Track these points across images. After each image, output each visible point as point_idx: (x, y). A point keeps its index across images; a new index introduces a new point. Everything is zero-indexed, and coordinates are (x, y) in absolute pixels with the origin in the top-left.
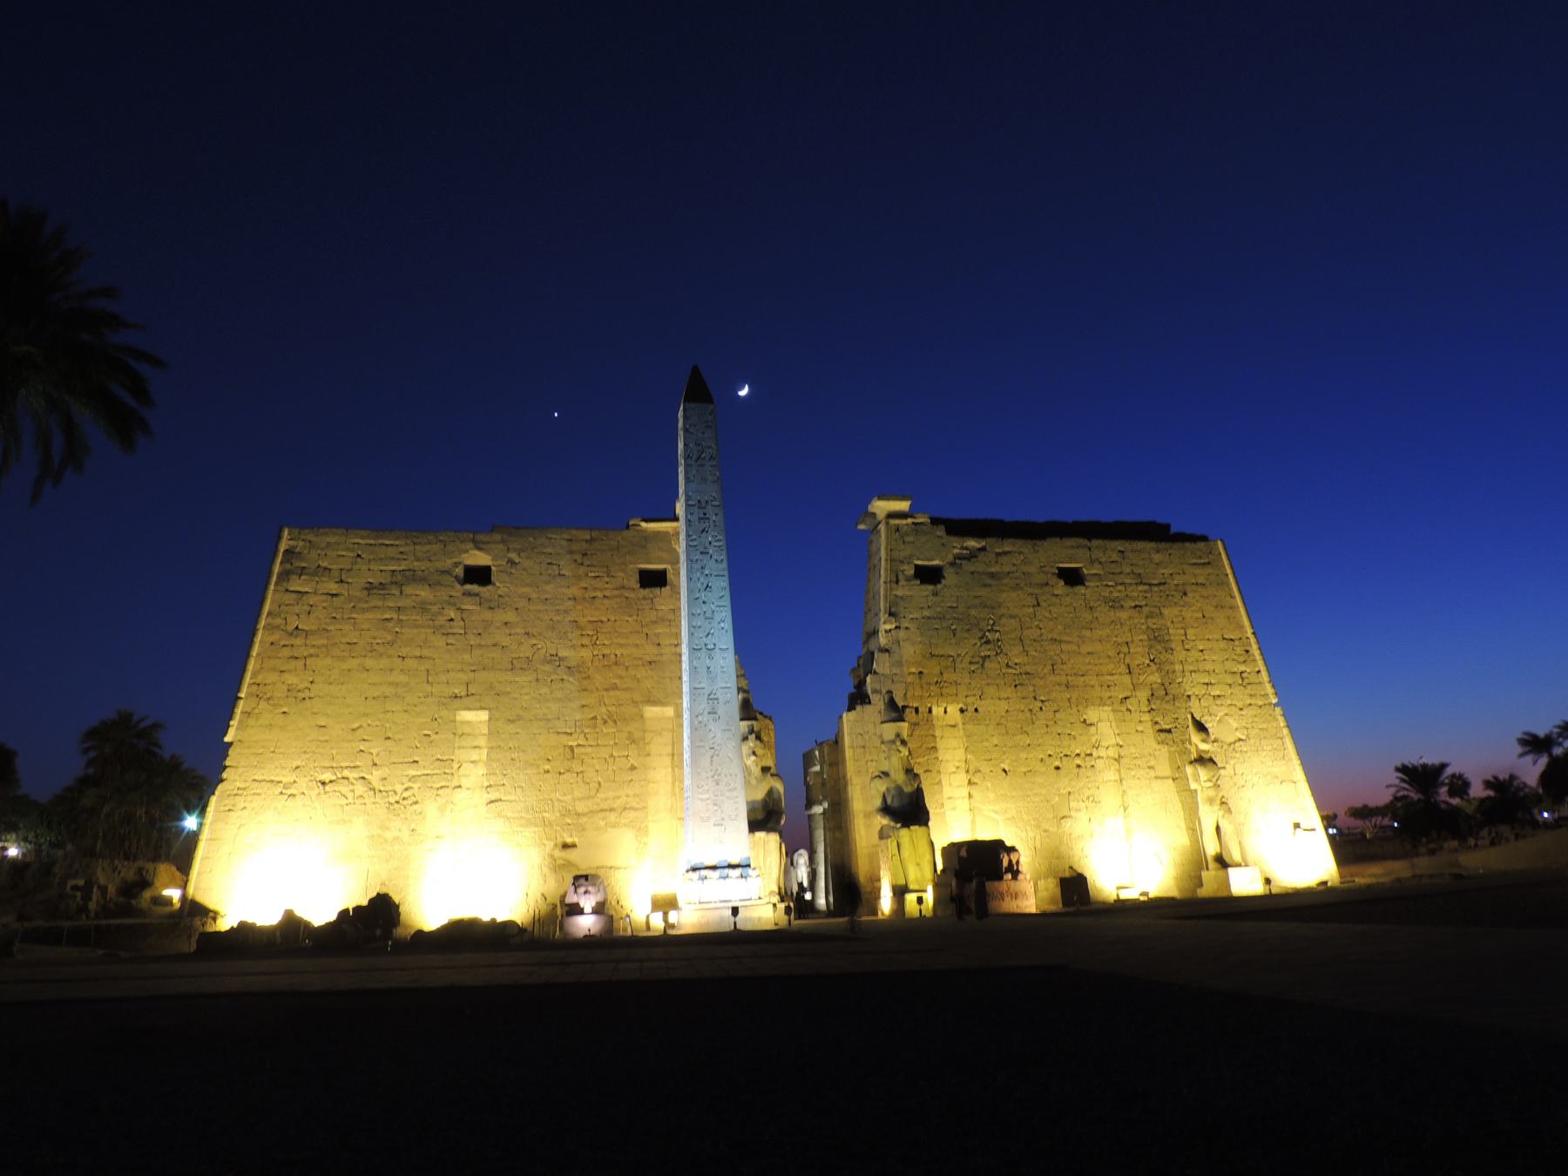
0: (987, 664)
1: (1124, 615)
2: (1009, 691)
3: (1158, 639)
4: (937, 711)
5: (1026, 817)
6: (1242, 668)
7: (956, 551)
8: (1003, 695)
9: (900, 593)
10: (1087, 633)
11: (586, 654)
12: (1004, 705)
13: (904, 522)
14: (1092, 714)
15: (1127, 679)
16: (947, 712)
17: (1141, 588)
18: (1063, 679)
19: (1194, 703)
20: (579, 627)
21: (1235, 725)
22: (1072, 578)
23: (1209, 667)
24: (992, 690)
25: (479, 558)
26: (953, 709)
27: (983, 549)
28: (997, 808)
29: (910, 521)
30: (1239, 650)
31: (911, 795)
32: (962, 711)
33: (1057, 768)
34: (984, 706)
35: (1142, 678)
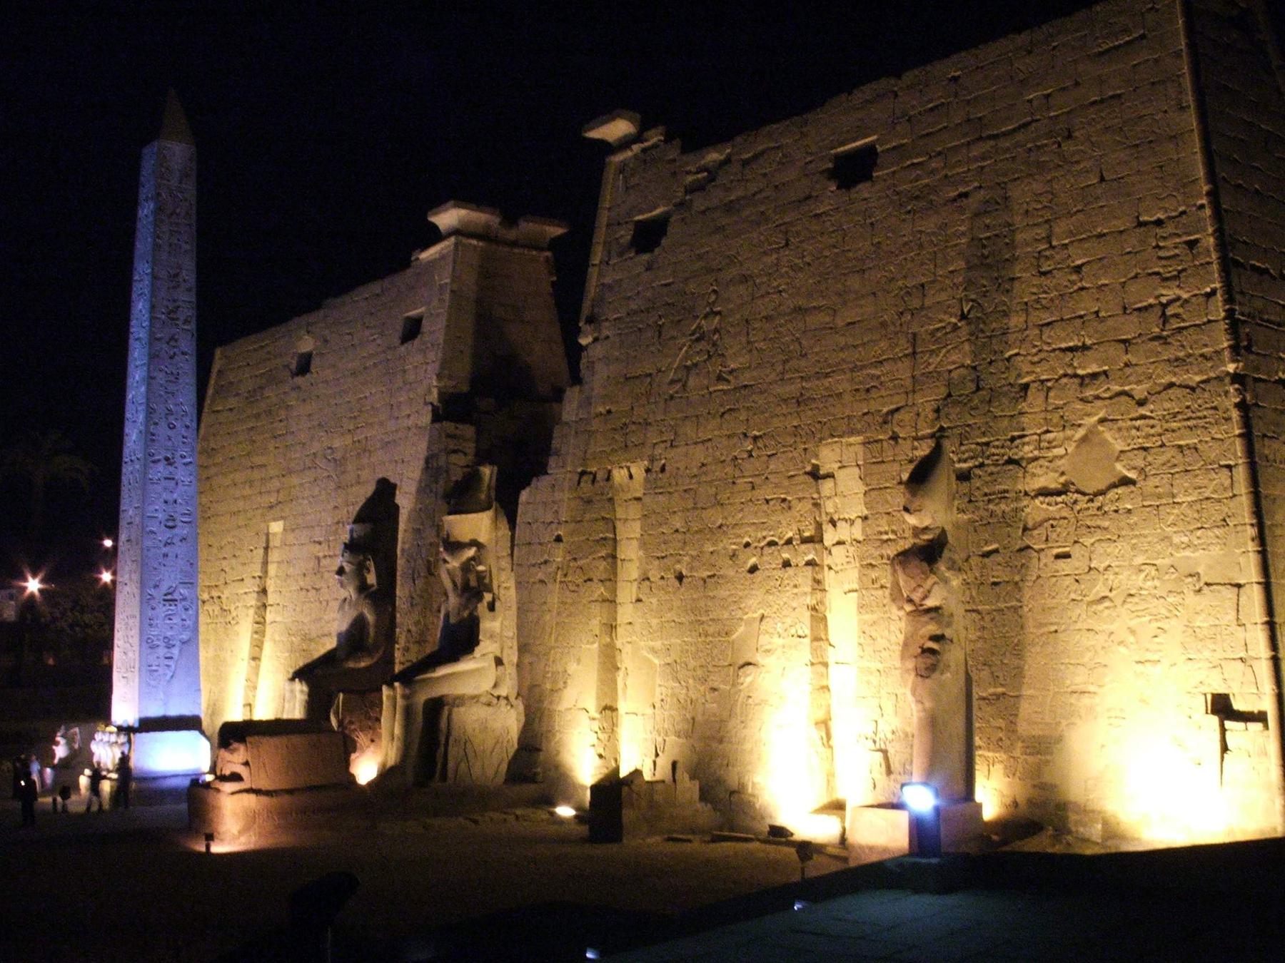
0: (692, 382)
1: (929, 224)
2: (711, 429)
3: (990, 264)
4: (619, 475)
5: (692, 663)
6: (1169, 293)
7: (690, 178)
8: (703, 437)
9: (607, 280)
10: (854, 282)
11: (348, 440)
12: (699, 454)
13: (629, 154)
14: (828, 457)
15: (903, 371)
16: (629, 475)
17: (976, 151)
18: (792, 389)
19: (1035, 400)
20: (351, 410)
21: (1119, 446)
22: (853, 170)
23: (1086, 305)
24: (689, 430)
25: (307, 345)
26: (638, 470)
27: (728, 161)
28: (658, 644)
29: (636, 148)
30: (1171, 246)
31: (461, 623)
32: (648, 471)
33: (753, 569)
34: (675, 458)
35: (935, 360)
